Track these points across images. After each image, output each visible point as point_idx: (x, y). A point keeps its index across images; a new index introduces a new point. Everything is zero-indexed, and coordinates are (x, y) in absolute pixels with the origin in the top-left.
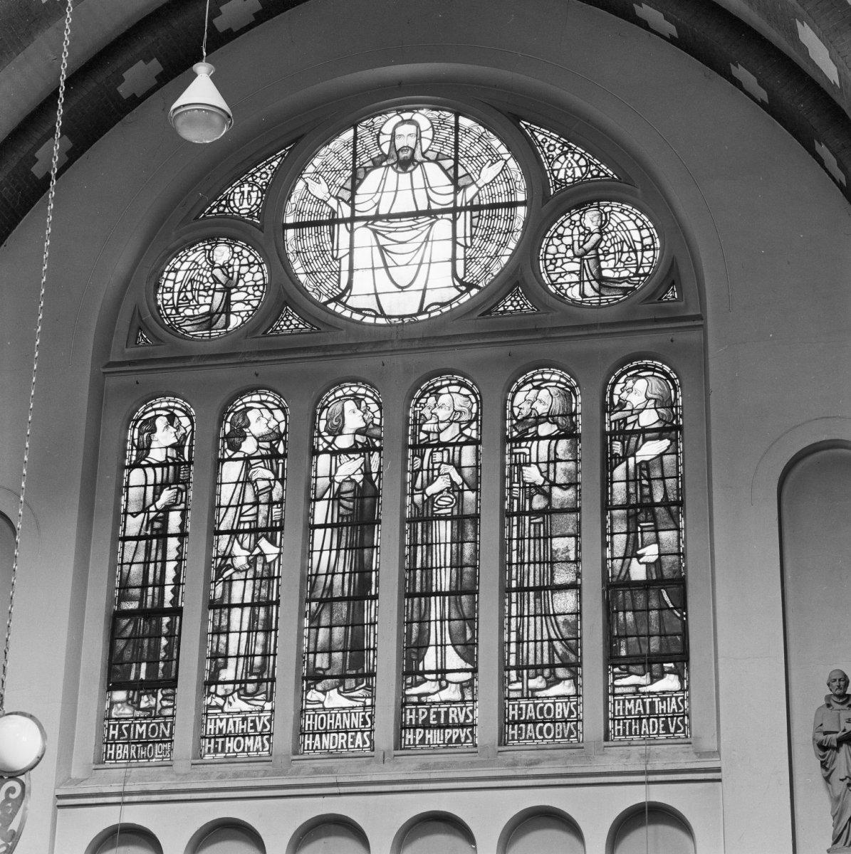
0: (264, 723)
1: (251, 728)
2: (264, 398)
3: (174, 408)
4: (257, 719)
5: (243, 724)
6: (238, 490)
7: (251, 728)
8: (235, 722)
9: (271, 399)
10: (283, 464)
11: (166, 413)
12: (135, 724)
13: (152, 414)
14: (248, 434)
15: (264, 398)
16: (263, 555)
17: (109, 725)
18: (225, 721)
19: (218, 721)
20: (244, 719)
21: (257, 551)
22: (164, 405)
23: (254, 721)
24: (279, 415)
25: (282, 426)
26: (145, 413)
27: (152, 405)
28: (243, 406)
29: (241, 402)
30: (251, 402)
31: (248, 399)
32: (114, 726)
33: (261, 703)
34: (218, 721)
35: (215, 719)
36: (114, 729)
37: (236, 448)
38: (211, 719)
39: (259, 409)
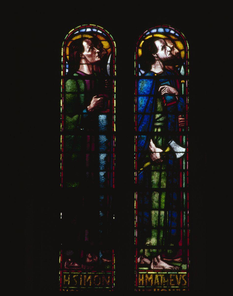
0: (182, 279)
1: (172, 283)
2: (167, 30)
3: (97, 33)
4: (177, 276)
5: (166, 280)
6: (151, 102)
7: (172, 283)
8: (159, 278)
9: (172, 32)
10: (185, 84)
11: (90, 37)
12: (83, 275)
13: (79, 37)
14: (156, 59)
15: (167, 30)
16: (173, 153)
17: (63, 275)
18: (152, 276)
19: (147, 276)
20: (167, 276)
21: (168, 150)
22: (89, 30)
23: (174, 278)
24: (180, 45)
25: (183, 53)
26: (73, 35)
27: (79, 29)
28: (151, 36)
29: (149, 33)
30: (157, 33)
31: (154, 31)
32: (67, 275)
33: (179, 265)
34: (147, 276)
35: (145, 275)
36: (67, 278)
37: (148, 69)
38: (141, 274)
39: (164, 39)
